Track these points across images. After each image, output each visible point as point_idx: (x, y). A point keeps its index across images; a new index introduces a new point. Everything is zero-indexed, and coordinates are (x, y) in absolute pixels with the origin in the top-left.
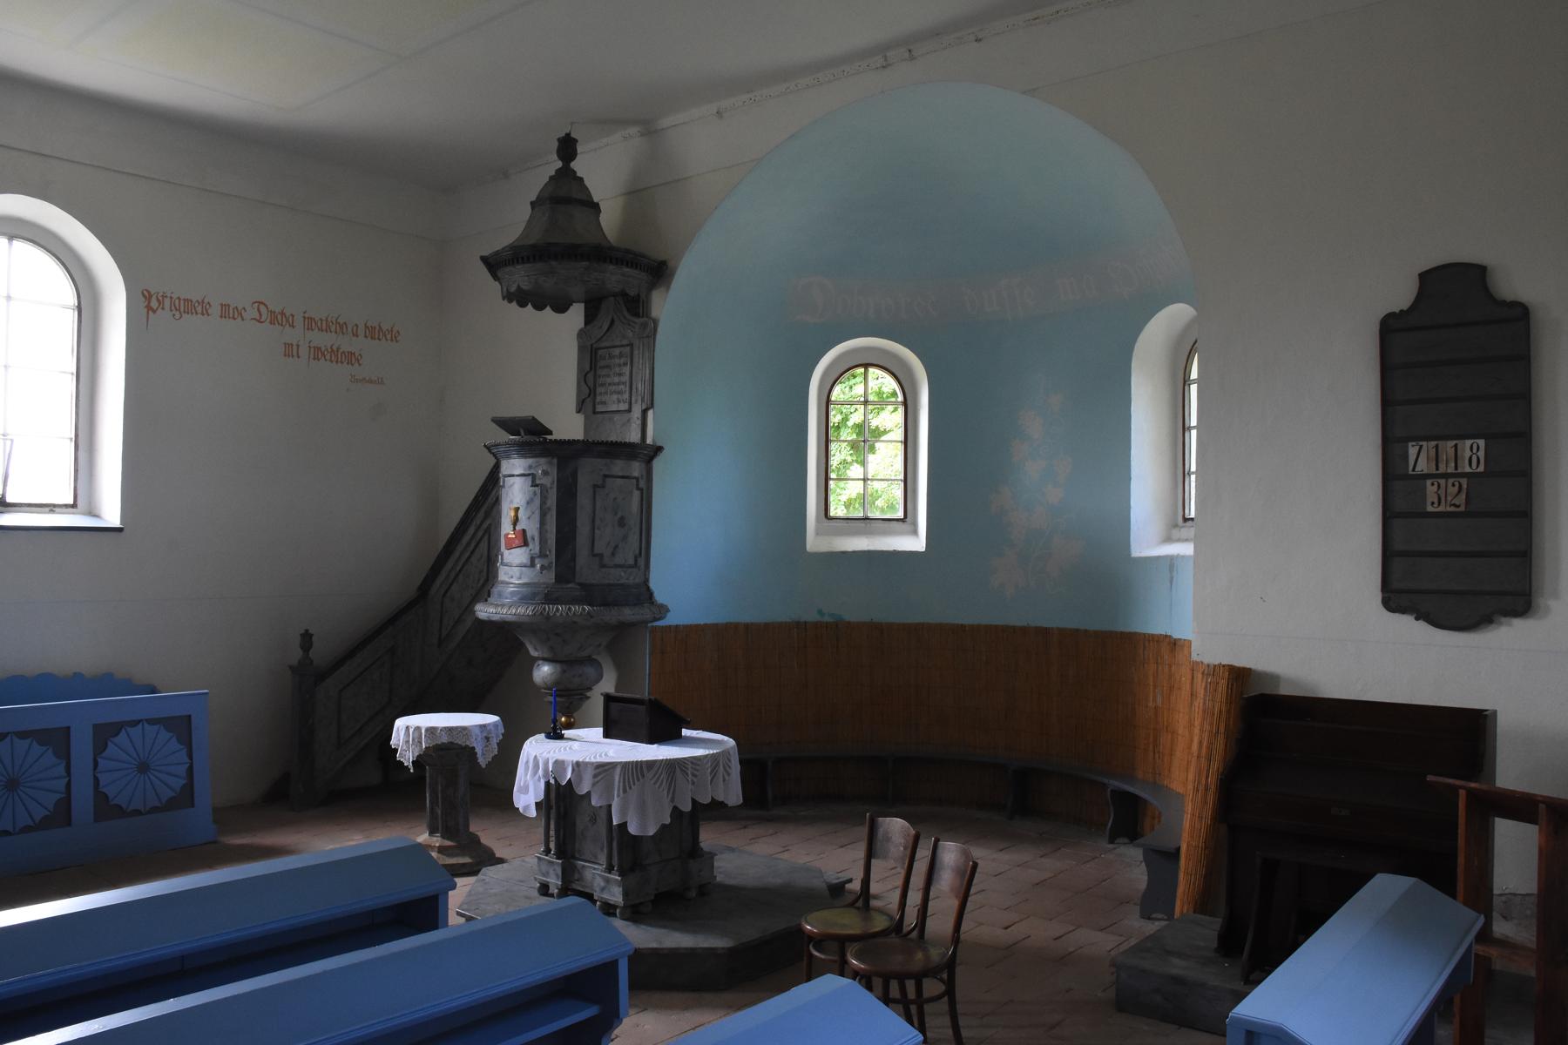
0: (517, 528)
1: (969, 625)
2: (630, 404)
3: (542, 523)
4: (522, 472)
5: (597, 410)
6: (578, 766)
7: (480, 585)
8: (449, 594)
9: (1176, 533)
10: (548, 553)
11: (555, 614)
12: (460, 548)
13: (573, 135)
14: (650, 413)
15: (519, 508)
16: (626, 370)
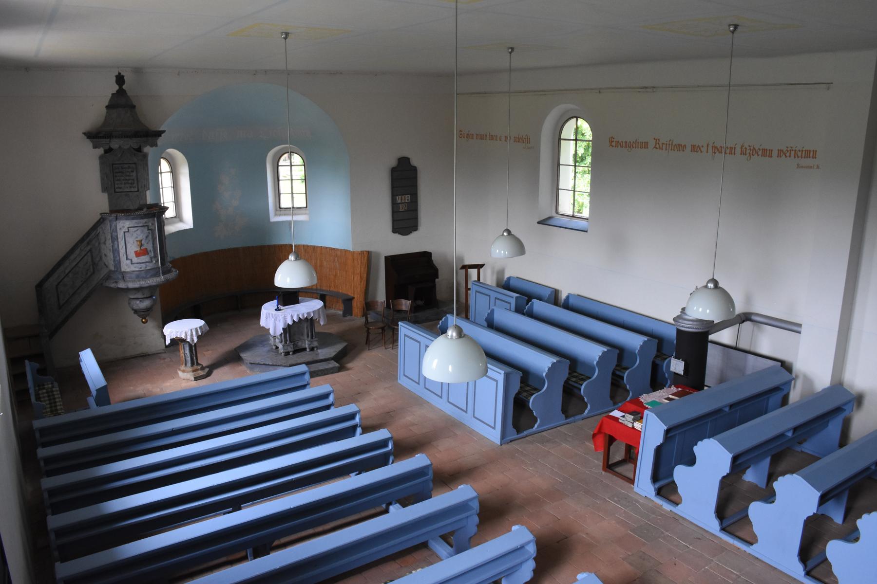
0: (142, 248)
2: (138, 188)
6: (314, 312)
9: (278, 213)
13: (122, 74)
15: (142, 240)
16: (135, 172)
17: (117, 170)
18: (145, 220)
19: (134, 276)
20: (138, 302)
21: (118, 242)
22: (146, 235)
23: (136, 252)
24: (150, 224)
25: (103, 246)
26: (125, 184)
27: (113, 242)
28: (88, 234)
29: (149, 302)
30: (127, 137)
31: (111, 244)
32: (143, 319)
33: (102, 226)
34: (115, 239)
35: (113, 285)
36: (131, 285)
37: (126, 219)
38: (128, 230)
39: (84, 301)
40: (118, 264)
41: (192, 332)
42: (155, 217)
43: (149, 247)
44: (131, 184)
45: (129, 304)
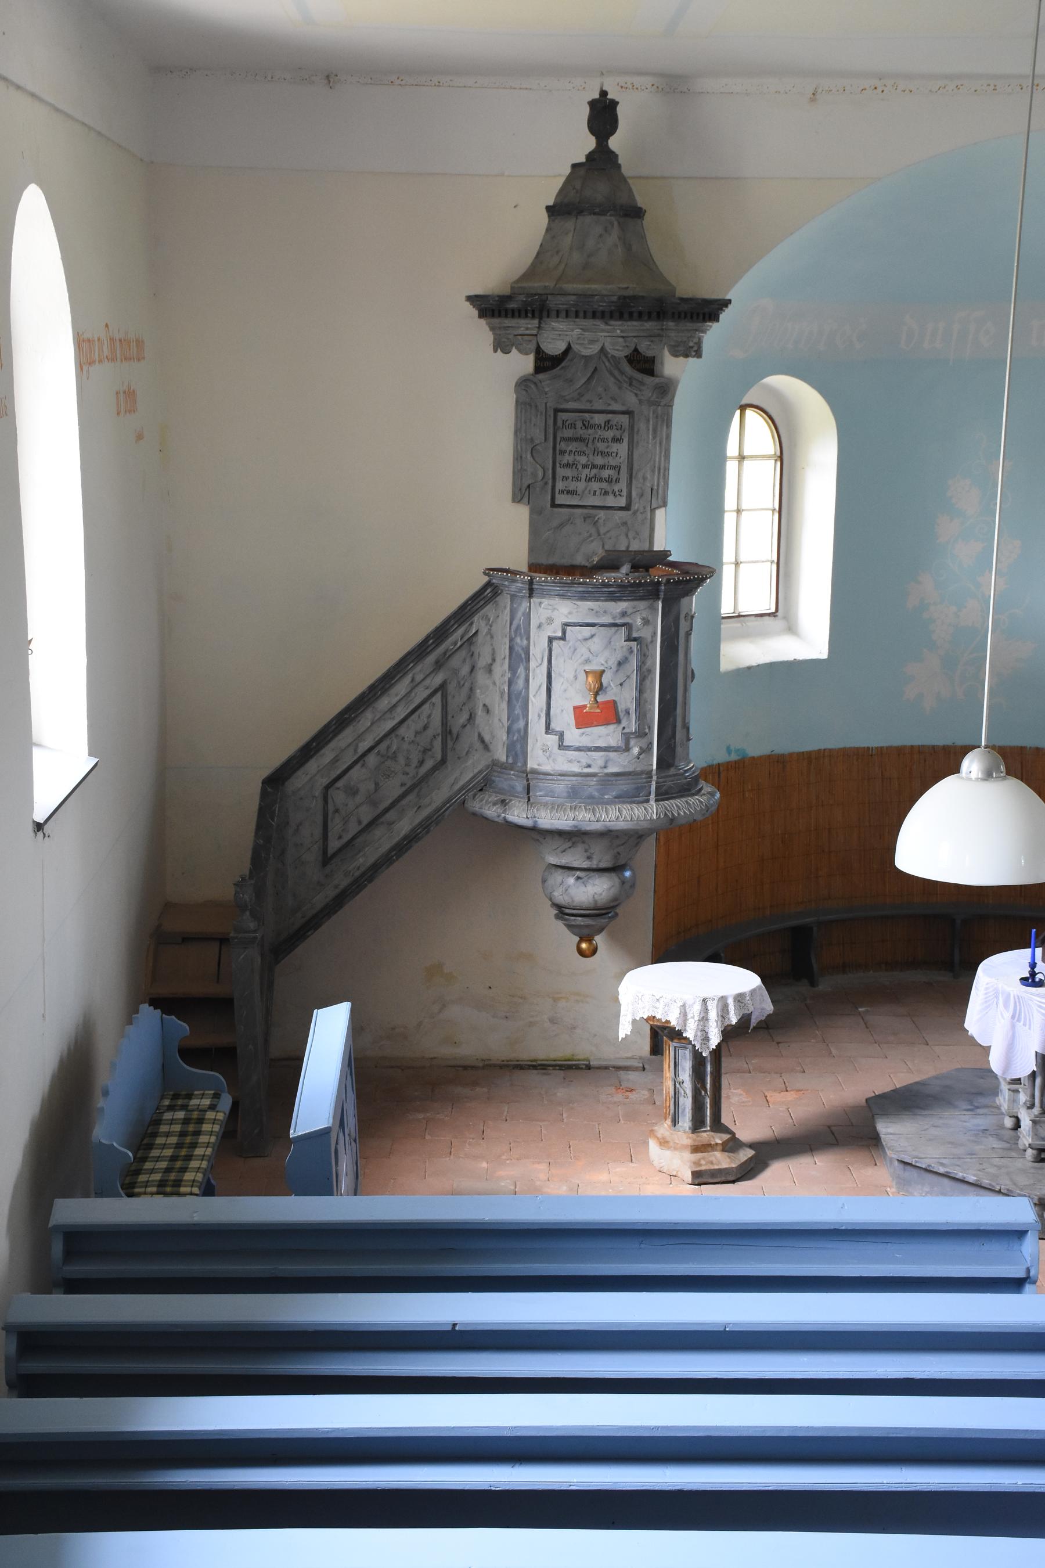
0: (599, 699)
1: (877, 748)
3: (641, 690)
4: (612, 621)
5: (558, 502)
7: (423, 770)
8: (340, 784)
10: (647, 730)
11: (679, 814)
12: (368, 717)
14: (660, 514)
15: (603, 672)
16: (623, 448)
17: (568, 433)
18: (623, 605)
19: (560, 787)
20: (571, 881)
21: (527, 669)
22: (619, 656)
23: (578, 710)
24: (639, 622)
25: (481, 677)
26: (589, 480)
27: (513, 669)
28: (441, 633)
29: (605, 886)
30: (594, 315)
31: (508, 675)
32: (581, 940)
33: (489, 610)
34: (519, 658)
35: (491, 812)
36: (547, 820)
37: (562, 596)
38: (564, 632)
39: (402, 848)
40: (518, 743)
41: (705, 1009)
42: (658, 599)
43: (626, 698)
44: (609, 481)
45: (544, 881)
